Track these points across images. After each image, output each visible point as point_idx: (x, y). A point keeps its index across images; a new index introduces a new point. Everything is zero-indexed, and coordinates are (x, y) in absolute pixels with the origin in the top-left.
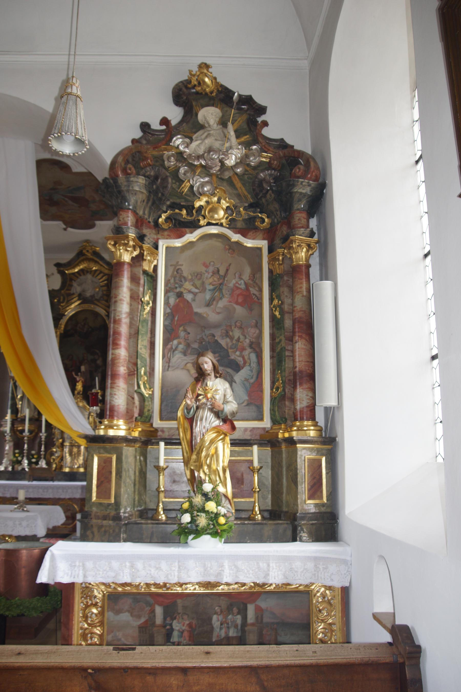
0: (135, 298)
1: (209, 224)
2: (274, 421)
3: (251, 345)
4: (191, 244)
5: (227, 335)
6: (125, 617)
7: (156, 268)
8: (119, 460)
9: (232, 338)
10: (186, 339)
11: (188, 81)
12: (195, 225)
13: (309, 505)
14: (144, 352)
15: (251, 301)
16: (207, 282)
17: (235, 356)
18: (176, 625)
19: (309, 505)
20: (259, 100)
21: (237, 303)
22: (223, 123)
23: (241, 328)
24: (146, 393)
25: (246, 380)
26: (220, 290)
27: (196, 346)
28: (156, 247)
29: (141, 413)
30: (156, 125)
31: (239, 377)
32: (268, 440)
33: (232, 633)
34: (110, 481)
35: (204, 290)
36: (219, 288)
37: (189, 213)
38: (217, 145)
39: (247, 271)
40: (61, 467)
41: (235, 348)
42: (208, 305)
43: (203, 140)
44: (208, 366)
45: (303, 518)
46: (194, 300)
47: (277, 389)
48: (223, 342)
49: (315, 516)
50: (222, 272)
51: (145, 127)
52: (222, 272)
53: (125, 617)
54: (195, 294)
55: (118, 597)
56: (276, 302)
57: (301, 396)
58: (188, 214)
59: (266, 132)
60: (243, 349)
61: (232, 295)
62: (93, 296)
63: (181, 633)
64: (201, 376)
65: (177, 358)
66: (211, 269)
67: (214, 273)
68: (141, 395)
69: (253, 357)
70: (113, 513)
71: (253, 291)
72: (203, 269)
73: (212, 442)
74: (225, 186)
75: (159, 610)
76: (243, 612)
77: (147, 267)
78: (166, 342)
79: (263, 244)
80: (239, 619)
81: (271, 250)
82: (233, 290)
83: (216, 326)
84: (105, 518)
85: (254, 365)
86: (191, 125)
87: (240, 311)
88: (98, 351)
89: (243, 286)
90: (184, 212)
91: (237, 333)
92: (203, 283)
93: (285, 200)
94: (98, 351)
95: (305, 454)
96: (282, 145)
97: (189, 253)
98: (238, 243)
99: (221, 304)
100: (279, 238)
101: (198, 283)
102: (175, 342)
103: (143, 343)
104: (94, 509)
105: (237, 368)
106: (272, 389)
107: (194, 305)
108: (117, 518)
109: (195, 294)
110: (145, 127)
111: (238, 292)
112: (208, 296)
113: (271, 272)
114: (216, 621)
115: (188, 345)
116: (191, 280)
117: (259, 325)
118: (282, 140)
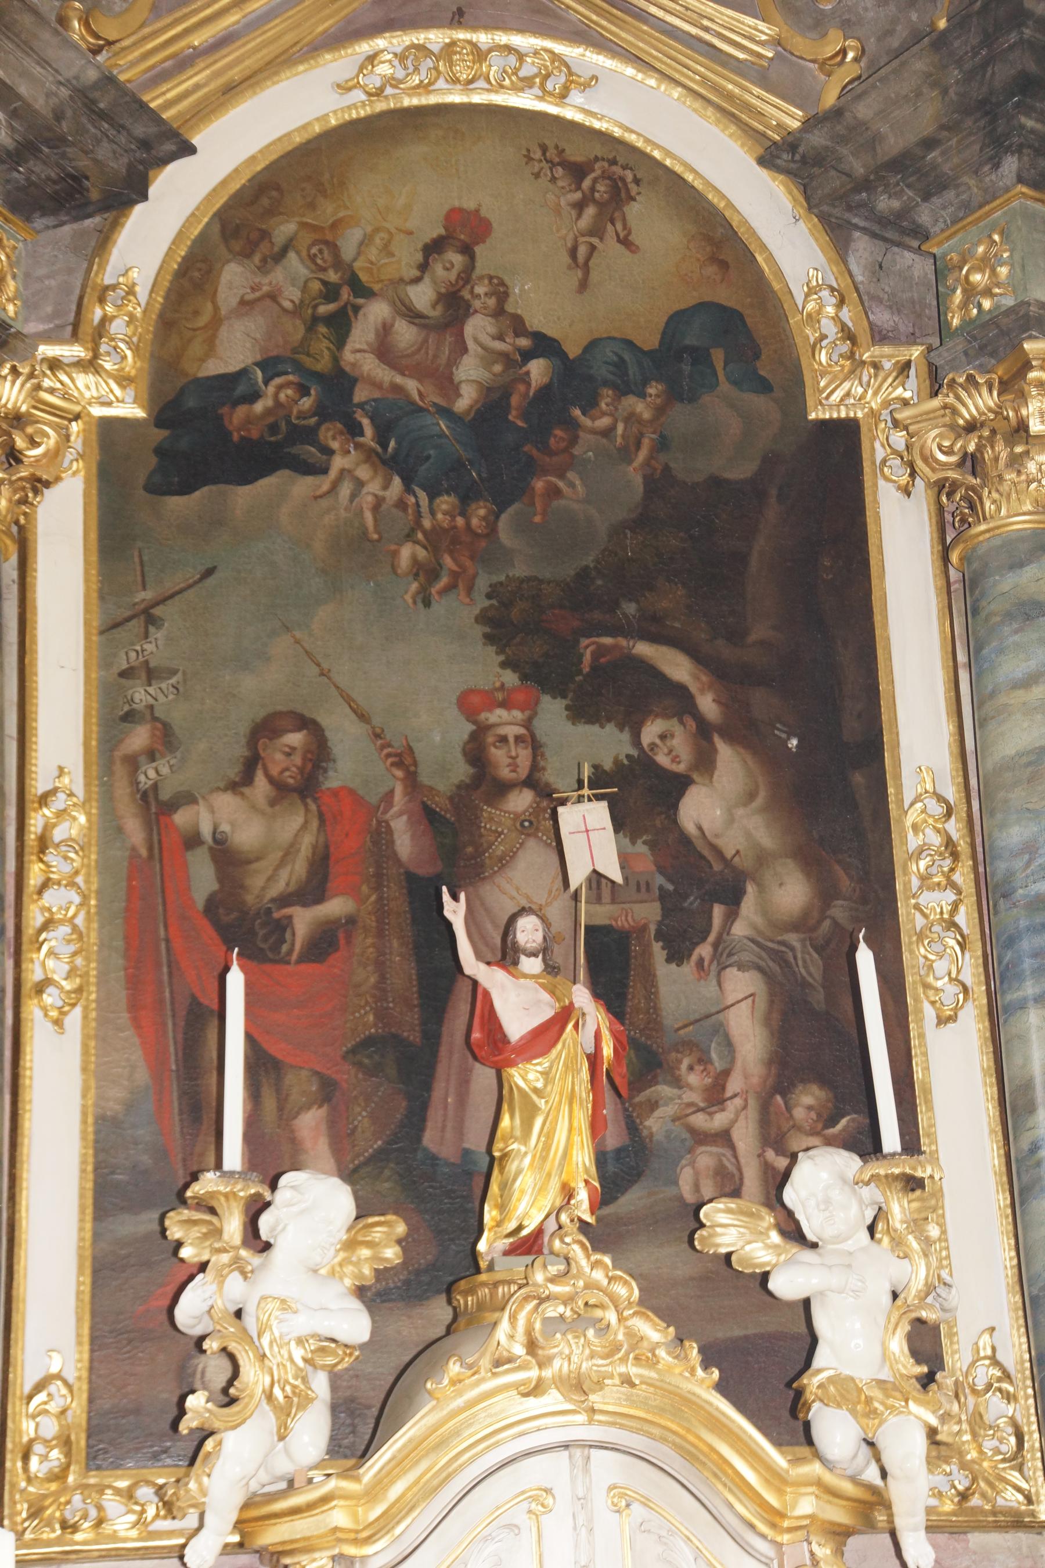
88: (678, 667)
94: (678, 667)
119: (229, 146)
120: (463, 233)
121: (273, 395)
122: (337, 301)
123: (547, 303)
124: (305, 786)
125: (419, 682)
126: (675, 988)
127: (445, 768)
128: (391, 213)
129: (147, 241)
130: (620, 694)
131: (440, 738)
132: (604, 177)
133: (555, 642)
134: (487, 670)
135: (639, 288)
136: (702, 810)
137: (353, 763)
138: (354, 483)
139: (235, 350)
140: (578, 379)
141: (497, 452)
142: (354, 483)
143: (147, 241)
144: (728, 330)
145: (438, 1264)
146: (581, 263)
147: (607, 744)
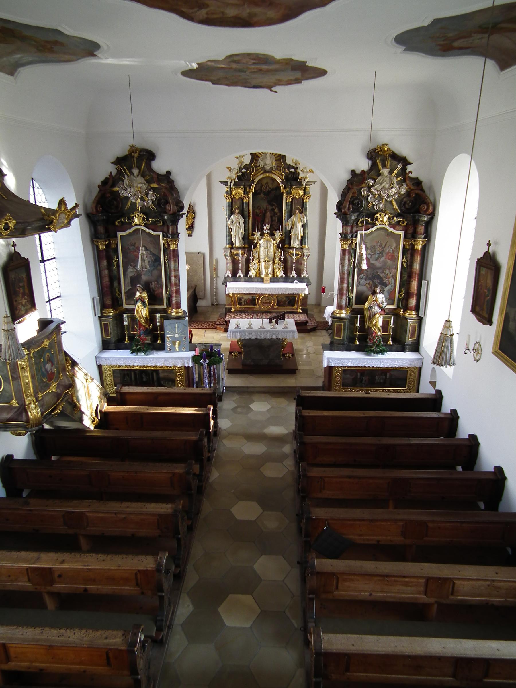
0: (350, 261)
1: (380, 224)
2: (398, 306)
3: (393, 276)
4: (372, 232)
5: (383, 272)
6: (348, 376)
7: (356, 244)
8: (345, 325)
9: (385, 273)
10: (367, 274)
11: (376, 149)
12: (374, 225)
13: (410, 340)
14: (351, 281)
15: (394, 258)
16: (377, 250)
17: (386, 280)
18: (364, 378)
19: (410, 340)
20: (410, 159)
21: (389, 259)
22: (391, 172)
23: (389, 269)
24: (351, 296)
25: (389, 290)
26: (382, 253)
27: (370, 276)
28: (356, 236)
29: (349, 304)
30: (358, 172)
31: (386, 289)
32: (394, 312)
33: (381, 381)
34: (341, 332)
35: (375, 254)
36: (381, 253)
37: (372, 220)
38: (387, 186)
39: (394, 245)
40: (259, 274)
41: (386, 277)
42: (377, 260)
43: (381, 184)
44: (378, 291)
45: (407, 345)
46: (371, 258)
47: (401, 295)
48: (381, 275)
49: (412, 344)
50: (383, 246)
51: (353, 172)
52: (383, 246)
53: (348, 376)
54: (371, 255)
55: (347, 371)
56: (404, 259)
57: (413, 302)
58: (371, 220)
59: (410, 175)
60: (389, 278)
61: (386, 255)
62: (271, 169)
63: (366, 380)
64: (374, 293)
65: (363, 281)
66: (379, 244)
67: (380, 246)
68: (350, 299)
69: (393, 281)
70: (342, 343)
71: (395, 253)
72: (376, 244)
73: (378, 318)
74: (389, 205)
75: (359, 374)
76: (386, 375)
77: (353, 246)
78: (358, 276)
79: (402, 233)
80: (384, 377)
81: (405, 237)
82: (387, 253)
83: (379, 268)
84: (339, 344)
85: (393, 284)
86: (374, 172)
87: (389, 262)
89: (392, 252)
90: (369, 219)
91: (387, 271)
92: (375, 250)
93: (415, 223)
95: (410, 323)
96: (417, 183)
97: (370, 237)
98: (391, 232)
99: (382, 259)
100: (411, 235)
101: (373, 250)
102: (362, 275)
103: (351, 277)
104: (335, 341)
105: (386, 285)
106: (399, 293)
107: (371, 260)
108: (343, 344)
109: (371, 255)
110: (353, 172)
111: (389, 254)
112: (377, 256)
113: (404, 245)
114: (377, 377)
115: (367, 276)
116: (370, 249)
117: (396, 268)
118: (417, 178)
119: (256, 180)
120: (267, 183)
121: (259, 191)
122: (262, 186)
123: (271, 186)
124: (260, 209)
125: (264, 205)
126: (274, 218)
127: (265, 209)
128: (265, 181)
129: (253, 186)
130: (273, 205)
131: (265, 207)
132: (274, 180)
133: (270, 203)
134: (267, 204)
135: (275, 185)
136: (275, 210)
137: (262, 208)
138: (262, 195)
139: (257, 189)
140: (272, 190)
141: (268, 194)
142: (262, 195)
143: (253, 186)
144: (279, 187)
145: (262, 235)
146: (272, 184)
147: (272, 207)
